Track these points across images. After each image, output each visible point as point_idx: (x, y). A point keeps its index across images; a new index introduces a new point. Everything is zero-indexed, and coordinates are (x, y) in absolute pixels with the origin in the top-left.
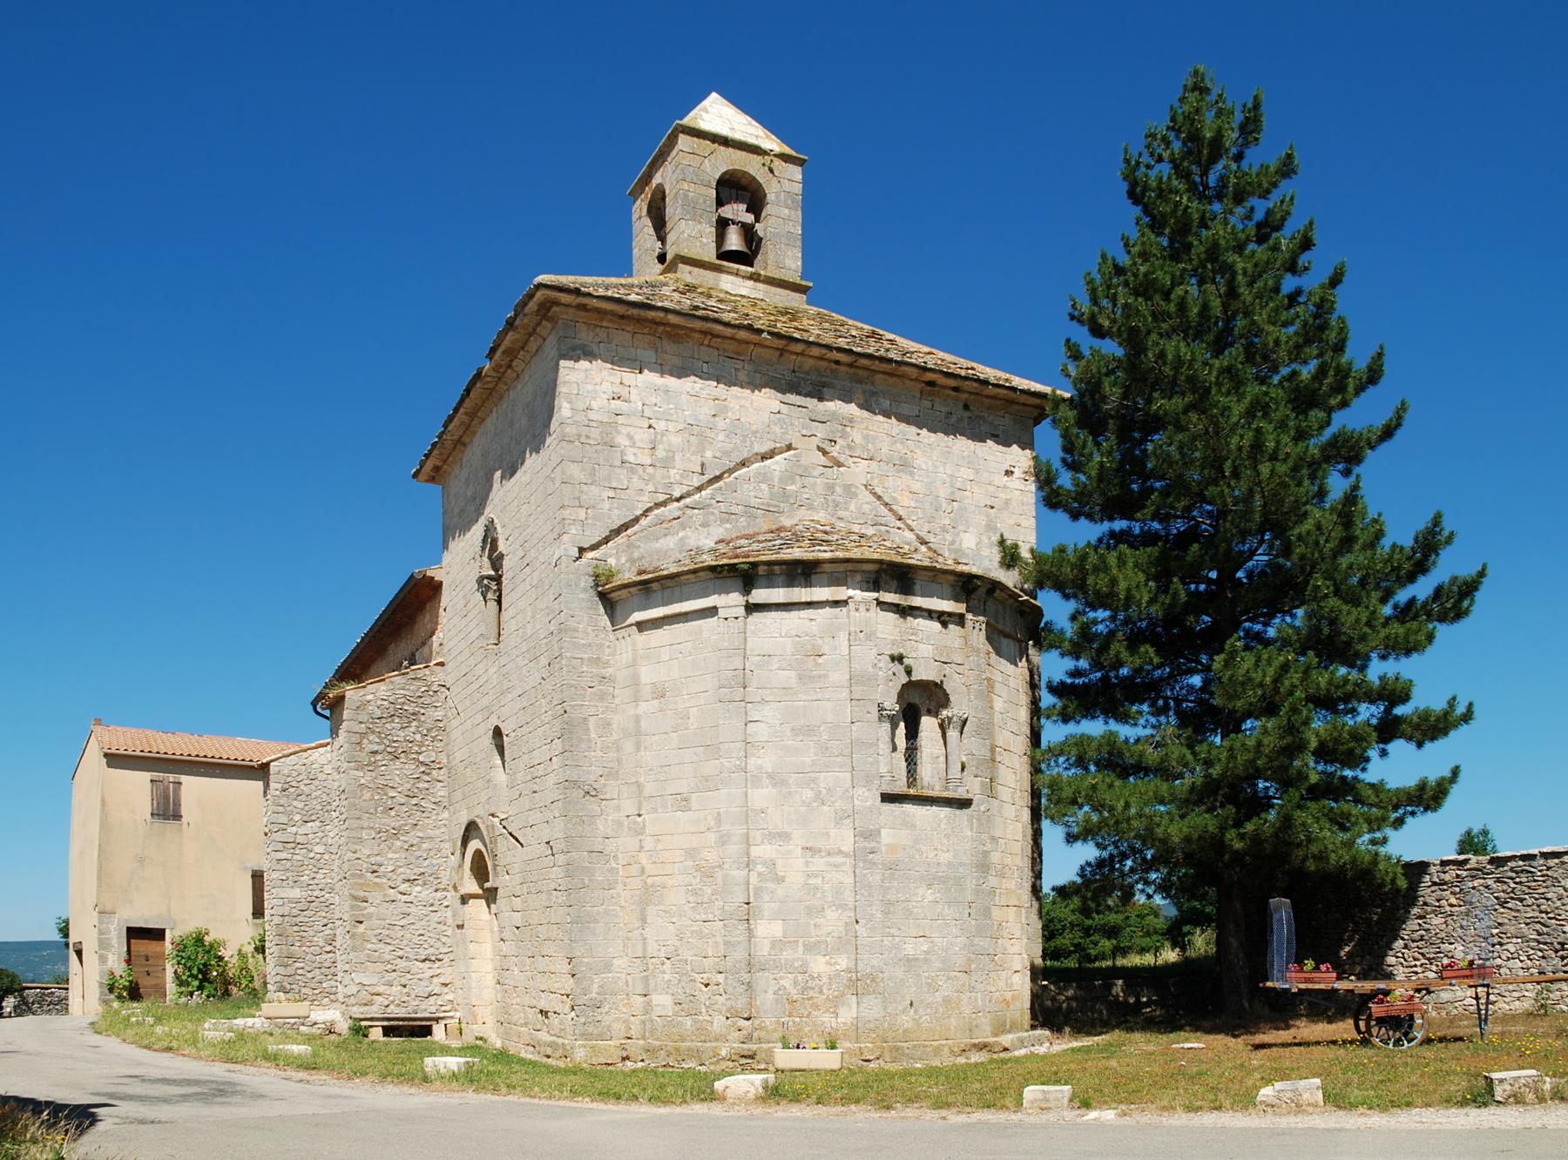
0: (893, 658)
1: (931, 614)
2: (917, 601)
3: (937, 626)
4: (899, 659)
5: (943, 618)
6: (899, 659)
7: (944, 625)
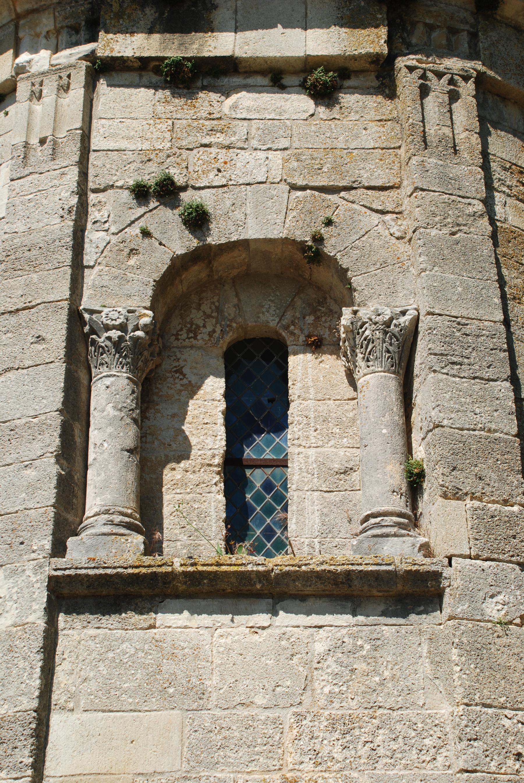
0: (141, 193)
1: (275, 75)
2: (222, 43)
3: (299, 103)
4: (167, 191)
5: (325, 81)
6: (167, 191)
7: (324, 95)
